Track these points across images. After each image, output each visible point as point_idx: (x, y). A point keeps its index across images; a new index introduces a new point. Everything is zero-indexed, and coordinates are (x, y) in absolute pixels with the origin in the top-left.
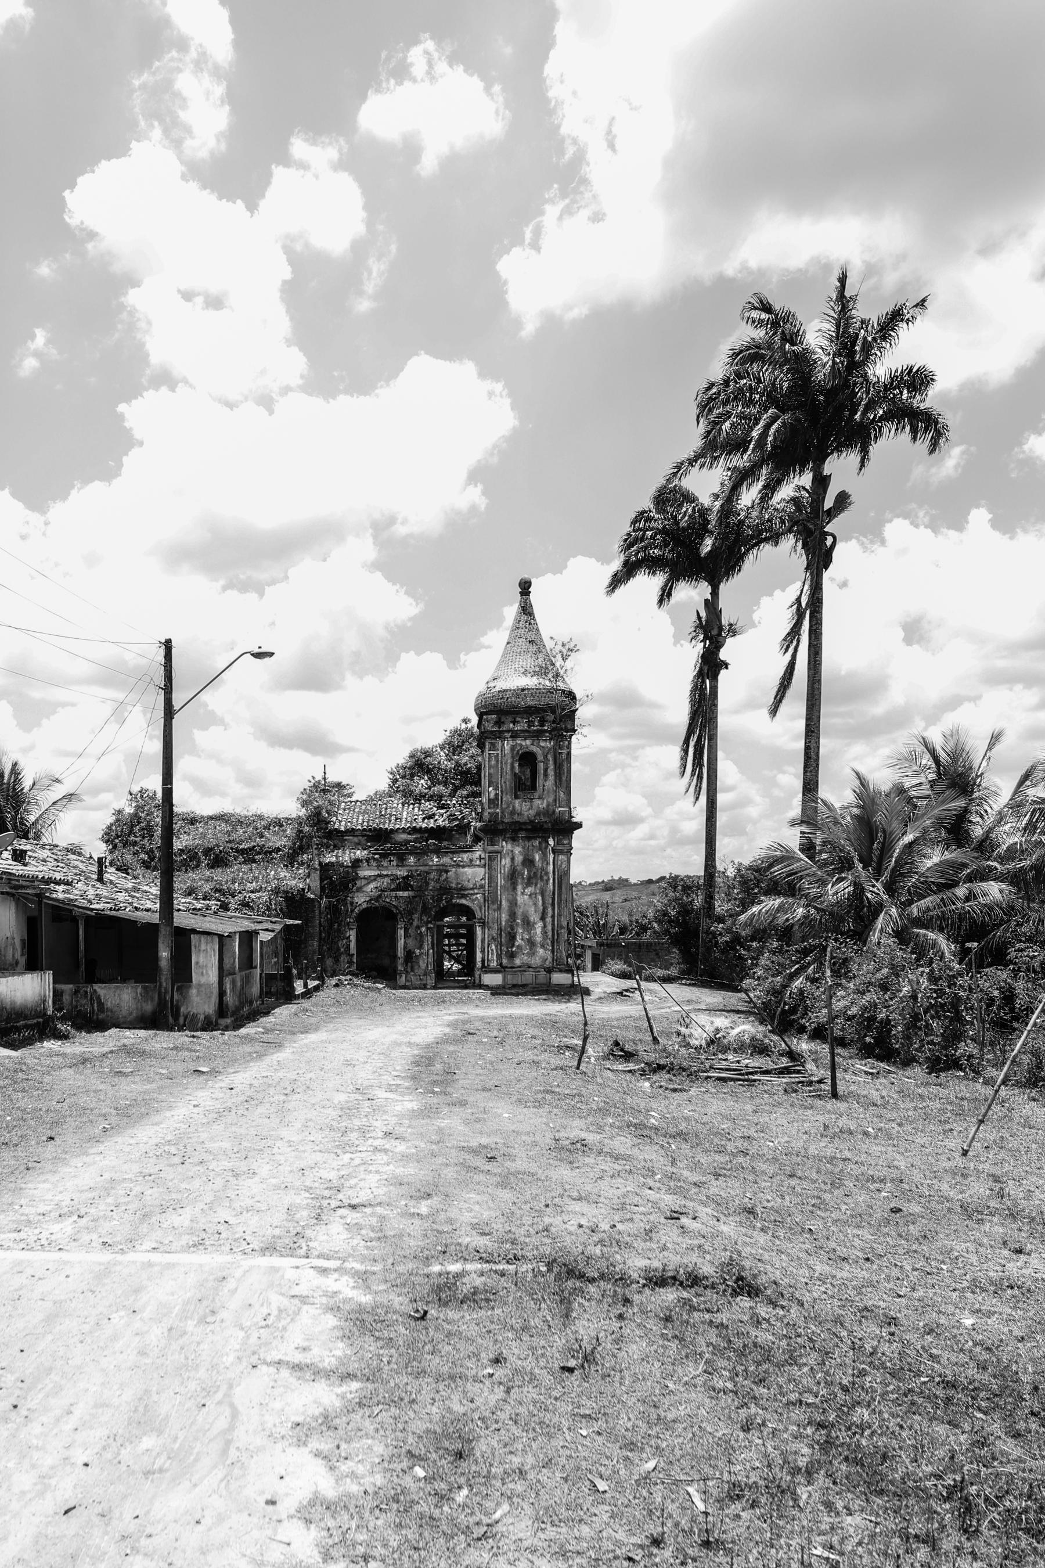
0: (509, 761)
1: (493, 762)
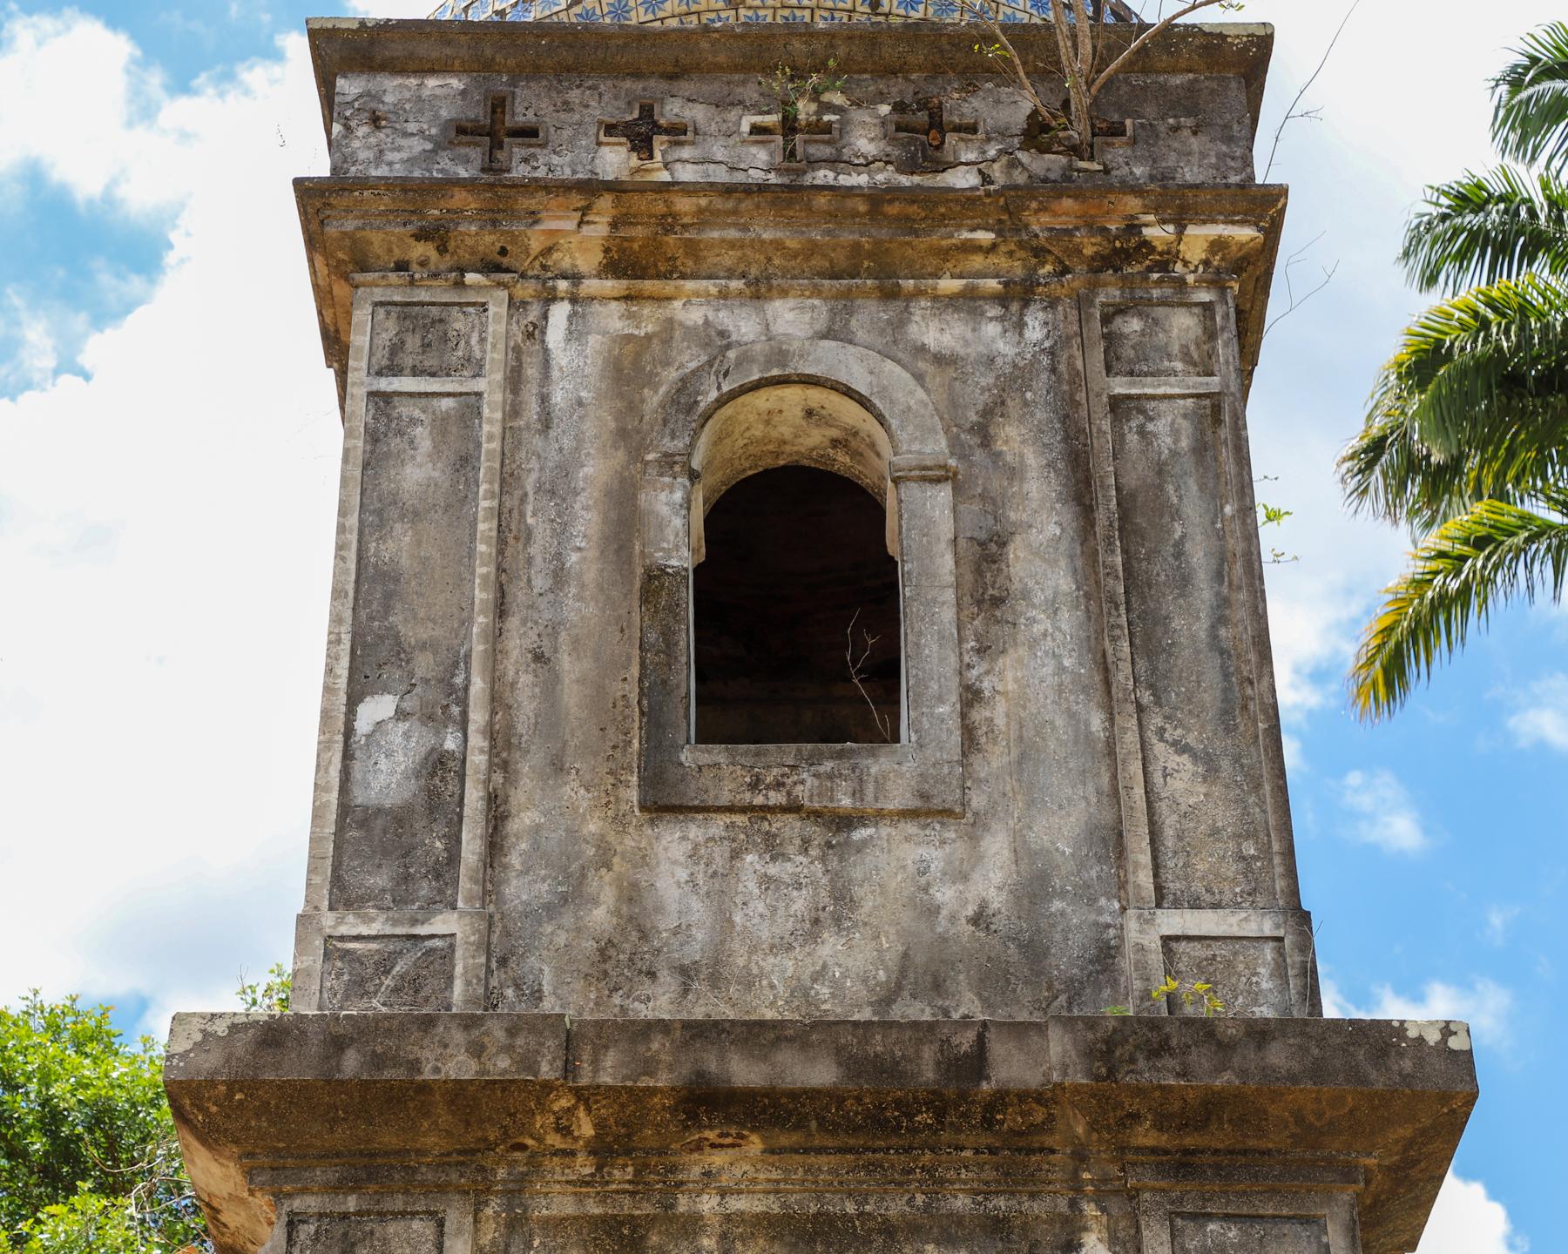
0: (595, 470)
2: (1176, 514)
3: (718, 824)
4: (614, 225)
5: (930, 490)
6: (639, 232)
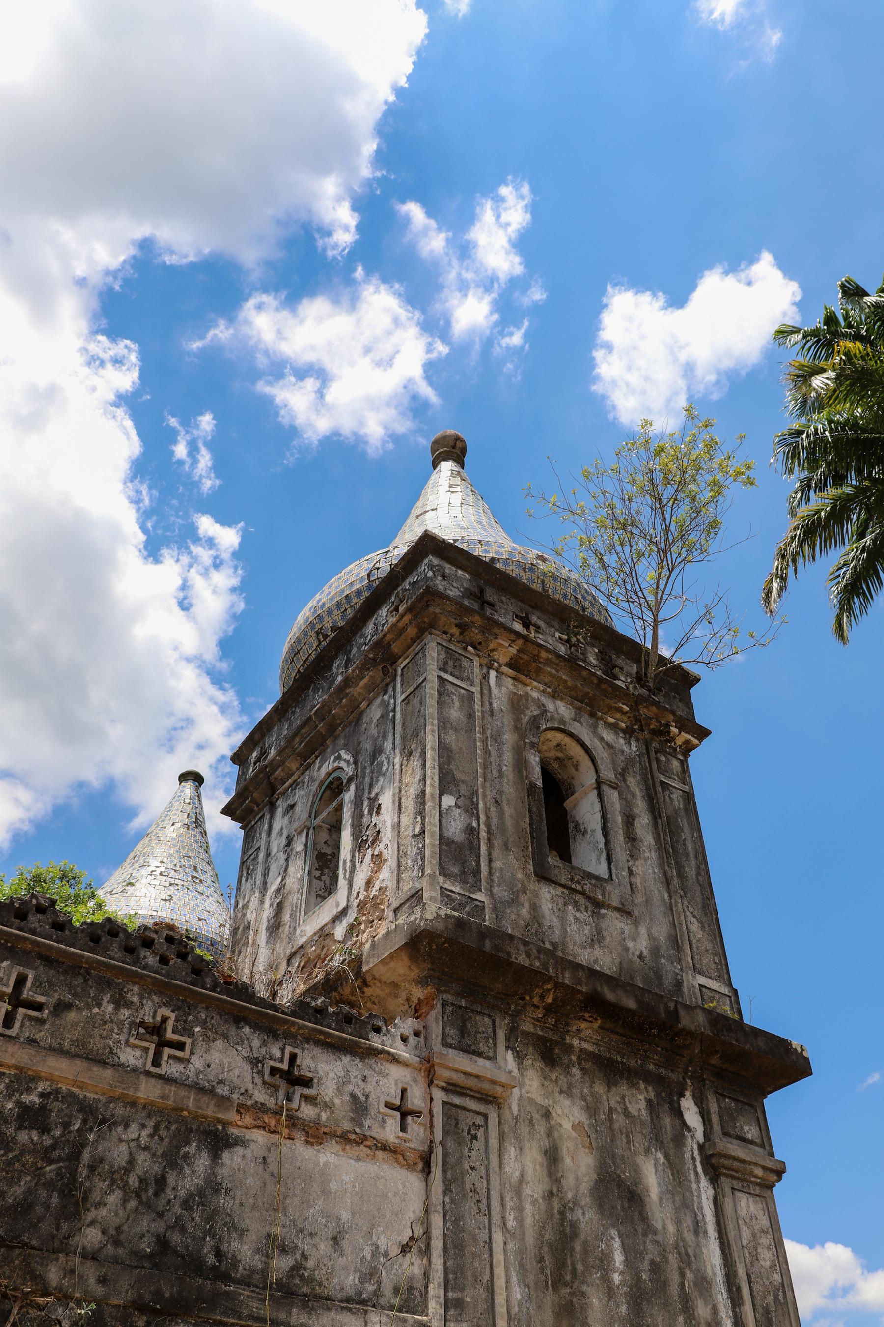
1: (455, 713)
2: (682, 831)
3: (560, 890)
4: (518, 651)
5: (612, 791)
6: (525, 657)
